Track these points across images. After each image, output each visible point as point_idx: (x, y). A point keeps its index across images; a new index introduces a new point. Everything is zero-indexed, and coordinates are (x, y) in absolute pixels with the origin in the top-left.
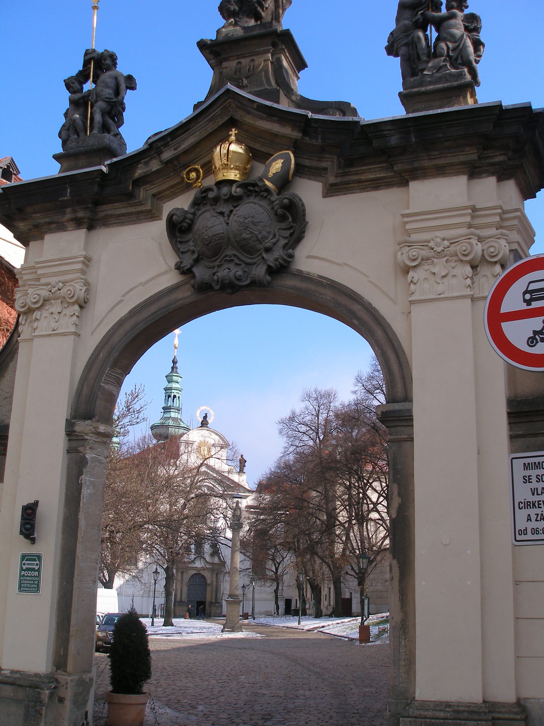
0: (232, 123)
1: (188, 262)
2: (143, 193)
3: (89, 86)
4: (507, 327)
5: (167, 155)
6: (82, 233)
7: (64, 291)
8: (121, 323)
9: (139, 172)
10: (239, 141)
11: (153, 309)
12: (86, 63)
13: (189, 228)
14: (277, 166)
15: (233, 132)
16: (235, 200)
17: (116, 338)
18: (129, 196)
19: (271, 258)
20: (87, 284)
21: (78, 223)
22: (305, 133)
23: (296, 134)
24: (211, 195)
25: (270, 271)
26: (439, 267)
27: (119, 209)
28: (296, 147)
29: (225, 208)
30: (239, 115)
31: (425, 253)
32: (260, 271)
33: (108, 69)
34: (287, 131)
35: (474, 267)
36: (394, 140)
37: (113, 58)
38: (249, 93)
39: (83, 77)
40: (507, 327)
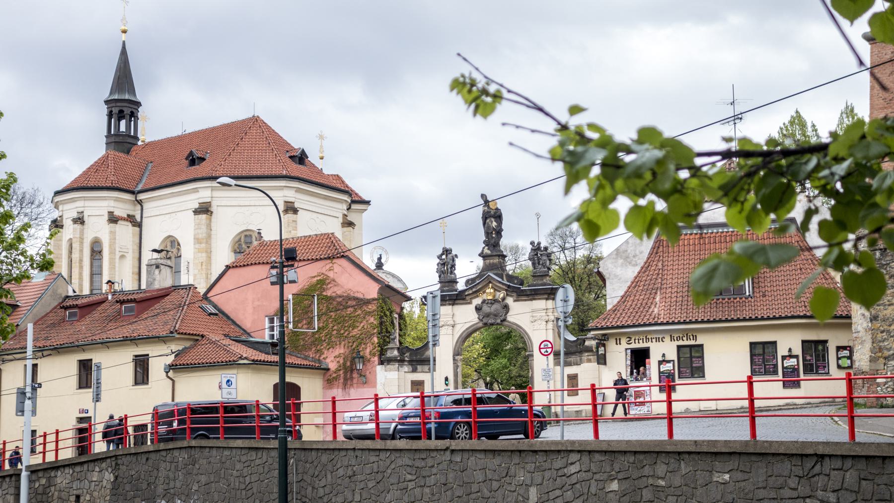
0: (490, 282)
1: (481, 318)
2: (467, 298)
3: (444, 257)
4: (541, 350)
5: (474, 290)
6: (451, 306)
7: (448, 323)
8: (464, 331)
9: (466, 293)
10: (492, 287)
11: (472, 328)
12: (443, 252)
13: (481, 309)
14: (502, 295)
15: (490, 285)
16: (492, 304)
17: (463, 335)
18: (464, 299)
19: (502, 318)
20: (454, 321)
21: (450, 304)
22: (508, 288)
23: (506, 288)
24: (486, 302)
25: (501, 321)
26: (539, 322)
27: (461, 302)
28: (506, 290)
29: (490, 305)
30: (492, 281)
31: (536, 319)
32: (499, 321)
33: (450, 253)
34: (504, 287)
35: (546, 322)
36: (528, 293)
37: (451, 250)
38: (494, 274)
39: (442, 254)
40: (541, 350)
